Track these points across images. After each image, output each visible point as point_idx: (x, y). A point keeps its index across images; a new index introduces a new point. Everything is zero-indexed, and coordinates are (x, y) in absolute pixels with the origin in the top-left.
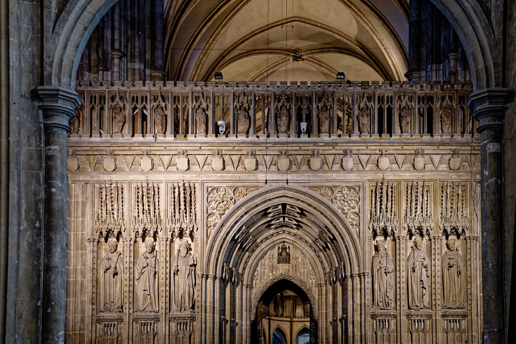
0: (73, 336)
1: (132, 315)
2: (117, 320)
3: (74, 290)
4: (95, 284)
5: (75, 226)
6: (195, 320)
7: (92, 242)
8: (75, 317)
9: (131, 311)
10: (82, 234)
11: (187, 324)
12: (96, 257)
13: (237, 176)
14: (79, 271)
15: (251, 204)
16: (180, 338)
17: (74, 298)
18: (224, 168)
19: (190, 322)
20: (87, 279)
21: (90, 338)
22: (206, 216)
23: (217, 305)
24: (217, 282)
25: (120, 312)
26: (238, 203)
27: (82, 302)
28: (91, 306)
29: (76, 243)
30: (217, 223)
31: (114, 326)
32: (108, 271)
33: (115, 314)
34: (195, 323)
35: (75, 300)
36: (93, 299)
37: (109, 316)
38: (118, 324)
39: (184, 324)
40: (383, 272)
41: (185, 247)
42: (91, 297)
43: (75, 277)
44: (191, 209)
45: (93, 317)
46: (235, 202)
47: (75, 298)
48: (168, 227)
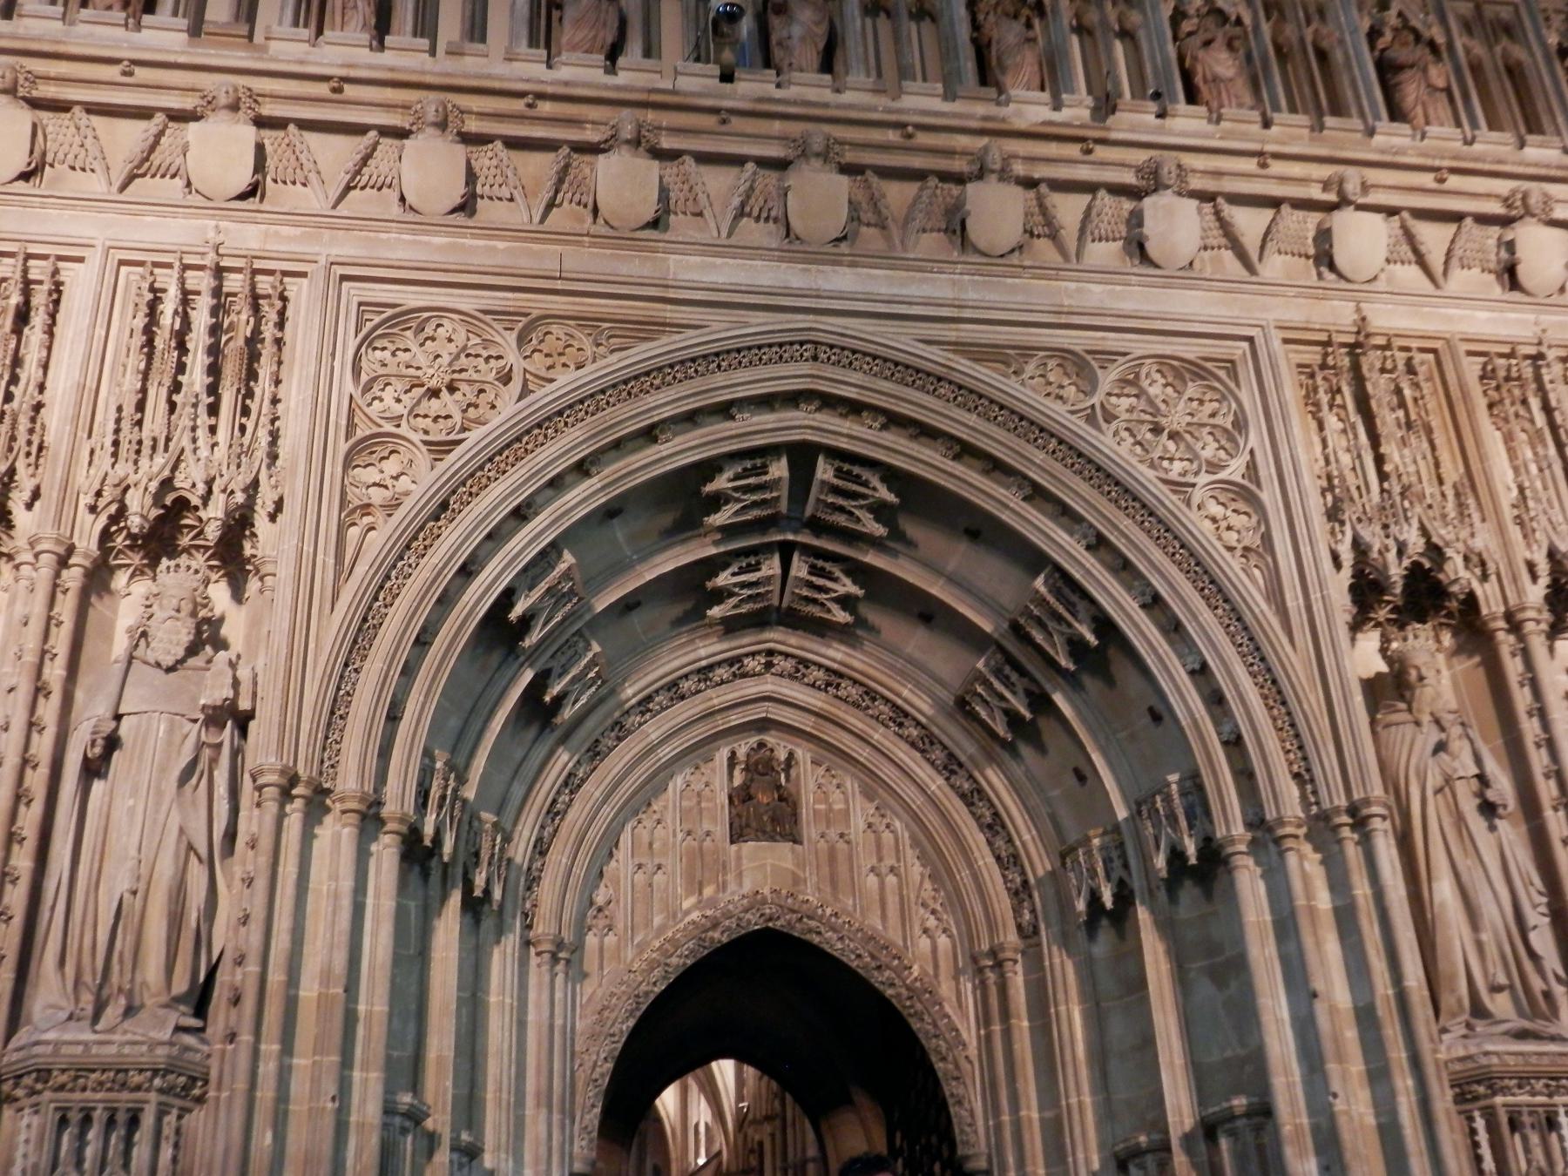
6: (200, 1100)
11: (134, 1122)
13: (544, 258)
15: (628, 415)
18: (467, 206)
19: (161, 1114)
22: (344, 447)
23: (374, 1002)
24: (386, 852)
26: (544, 396)
30: (407, 494)
34: (197, 1119)
39: (111, 1123)
40: (1469, 806)
41: (187, 607)
44: (250, 394)
46: (525, 392)
48: (86, 481)
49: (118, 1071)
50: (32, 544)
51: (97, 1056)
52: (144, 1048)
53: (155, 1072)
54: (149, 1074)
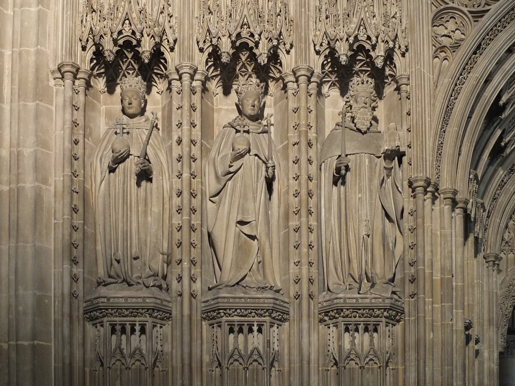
0: (13, 355)
1: (199, 297)
2: (151, 311)
3: (14, 217)
4: (78, 201)
5: (18, 29)
7: (68, 75)
8: (17, 296)
9: (197, 286)
10: (38, 53)
12: (81, 121)
14: (28, 163)
16: (352, 370)
17: (13, 241)
20: (52, 188)
21: (67, 361)
25: (160, 287)
27: (38, 253)
28: (67, 266)
29: (20, 81)
31: (143, 331)
32: (121, 166)
33: (144, 293)
35: (17, 248)
36: (73, 245)
37: (126, 298)
38: (154, 326)
42: (67, 237)
43: (14, 178)
45: (76, 301)
47: (17, 242)
49: (370, 309)
50: (294, 73)
51: (361, 303)
52: (381, 300)
53: (385, 310)
54: (382, 310)
